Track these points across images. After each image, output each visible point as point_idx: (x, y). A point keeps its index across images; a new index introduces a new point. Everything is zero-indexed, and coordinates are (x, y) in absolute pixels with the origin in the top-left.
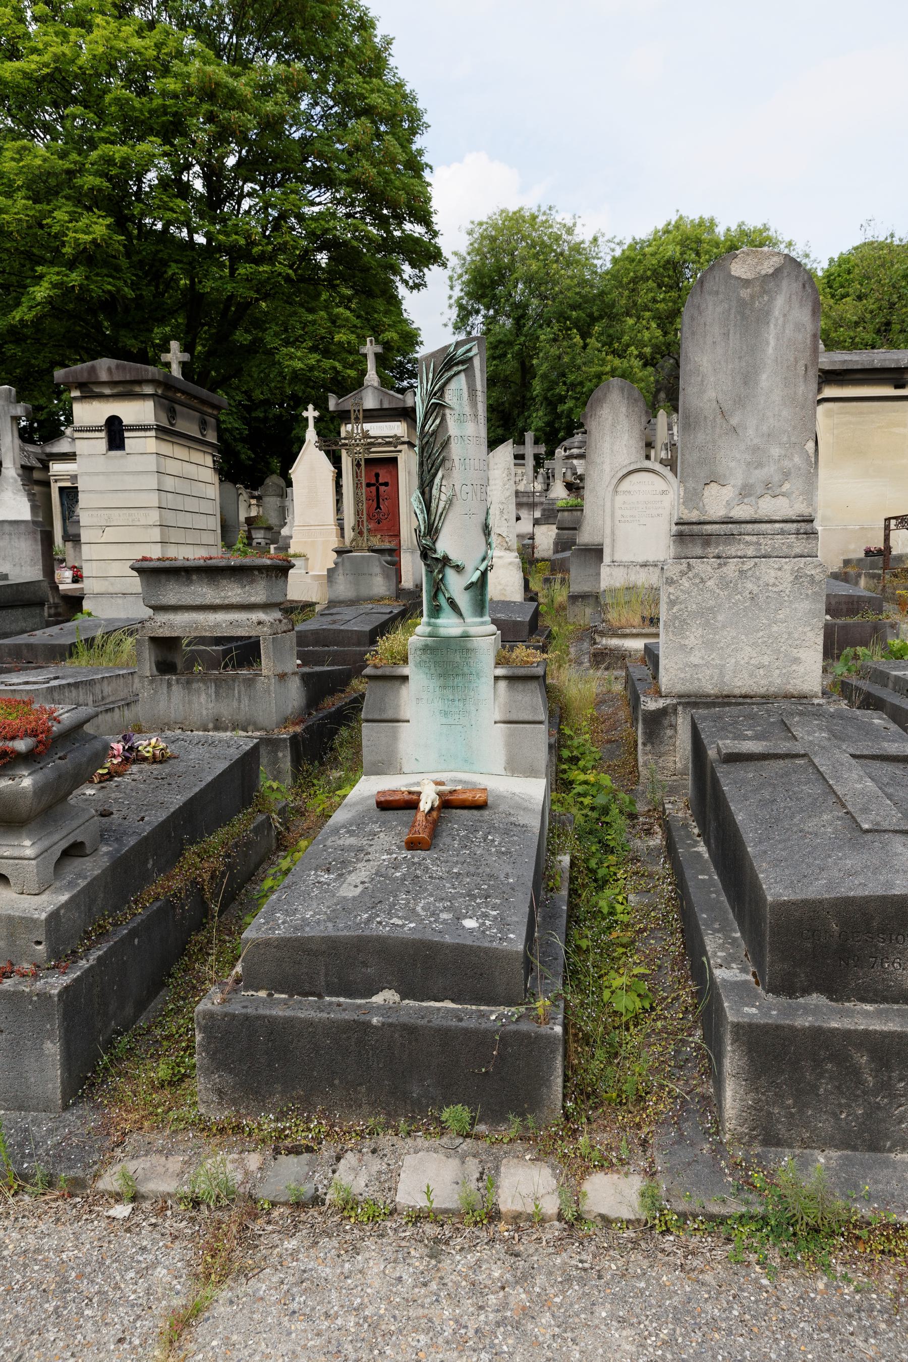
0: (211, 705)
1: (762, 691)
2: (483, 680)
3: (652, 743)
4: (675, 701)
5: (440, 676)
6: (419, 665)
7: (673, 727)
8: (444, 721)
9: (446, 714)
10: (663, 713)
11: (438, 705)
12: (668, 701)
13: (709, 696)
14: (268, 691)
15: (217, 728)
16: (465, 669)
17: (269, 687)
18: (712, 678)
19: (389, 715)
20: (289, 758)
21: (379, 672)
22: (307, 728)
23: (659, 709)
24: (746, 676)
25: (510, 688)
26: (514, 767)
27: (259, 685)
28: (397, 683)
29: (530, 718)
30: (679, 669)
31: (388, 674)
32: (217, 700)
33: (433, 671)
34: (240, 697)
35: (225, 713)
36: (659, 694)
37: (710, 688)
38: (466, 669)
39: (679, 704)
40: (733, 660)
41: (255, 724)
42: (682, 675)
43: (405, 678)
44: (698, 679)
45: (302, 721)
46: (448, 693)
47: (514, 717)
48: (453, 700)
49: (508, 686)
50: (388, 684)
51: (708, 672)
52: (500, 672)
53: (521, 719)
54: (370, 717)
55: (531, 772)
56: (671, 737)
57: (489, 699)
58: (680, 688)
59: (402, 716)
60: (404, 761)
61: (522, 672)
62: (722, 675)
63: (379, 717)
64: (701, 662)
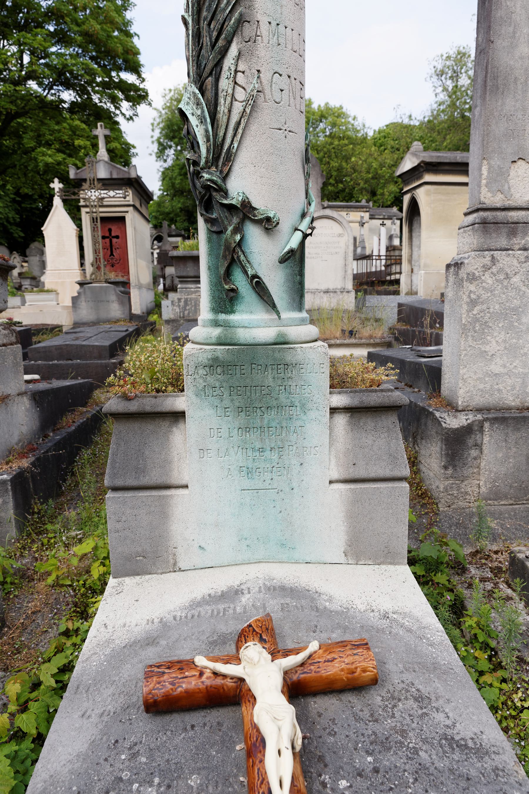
2: (312, 414)
3: (454, 467)
4: (479, 417)
5: (240, 410)
7: (479, 446)
8: (246, 483)
9: (249, 472)
10: (468, 430)
11: (236, 458)
12: (471, 417)
13: (509, 409)
18: (513, 388)
20: (11, 504)
21: (133, 407)
22: (38, 459)
23: (463, 427)
25: (353, 426)
26: (361, 549)
28: (165, 424)
30: (478, 379)
31: (148, 409)
33: (227, 402)
36: (452, 407)
37: (511, 400)
38: (283, 398)
42: (481, 386)
43: (179, 416)
44: (499, 390)
45: (33, 450)
46: (253, 437)
47: (362, 473)
48: (261, 450)
49: (350, 423)
50: (149, 427)
51: (510, 382)
52: (339, 400)
54: (119, 483)
55: (385, 557)
56: (475, 459)
57: (322, 444)
58: (479, 401)
59: (175, 479)
60: (180, 551)
61: (374, 399)
64: (502, 370)
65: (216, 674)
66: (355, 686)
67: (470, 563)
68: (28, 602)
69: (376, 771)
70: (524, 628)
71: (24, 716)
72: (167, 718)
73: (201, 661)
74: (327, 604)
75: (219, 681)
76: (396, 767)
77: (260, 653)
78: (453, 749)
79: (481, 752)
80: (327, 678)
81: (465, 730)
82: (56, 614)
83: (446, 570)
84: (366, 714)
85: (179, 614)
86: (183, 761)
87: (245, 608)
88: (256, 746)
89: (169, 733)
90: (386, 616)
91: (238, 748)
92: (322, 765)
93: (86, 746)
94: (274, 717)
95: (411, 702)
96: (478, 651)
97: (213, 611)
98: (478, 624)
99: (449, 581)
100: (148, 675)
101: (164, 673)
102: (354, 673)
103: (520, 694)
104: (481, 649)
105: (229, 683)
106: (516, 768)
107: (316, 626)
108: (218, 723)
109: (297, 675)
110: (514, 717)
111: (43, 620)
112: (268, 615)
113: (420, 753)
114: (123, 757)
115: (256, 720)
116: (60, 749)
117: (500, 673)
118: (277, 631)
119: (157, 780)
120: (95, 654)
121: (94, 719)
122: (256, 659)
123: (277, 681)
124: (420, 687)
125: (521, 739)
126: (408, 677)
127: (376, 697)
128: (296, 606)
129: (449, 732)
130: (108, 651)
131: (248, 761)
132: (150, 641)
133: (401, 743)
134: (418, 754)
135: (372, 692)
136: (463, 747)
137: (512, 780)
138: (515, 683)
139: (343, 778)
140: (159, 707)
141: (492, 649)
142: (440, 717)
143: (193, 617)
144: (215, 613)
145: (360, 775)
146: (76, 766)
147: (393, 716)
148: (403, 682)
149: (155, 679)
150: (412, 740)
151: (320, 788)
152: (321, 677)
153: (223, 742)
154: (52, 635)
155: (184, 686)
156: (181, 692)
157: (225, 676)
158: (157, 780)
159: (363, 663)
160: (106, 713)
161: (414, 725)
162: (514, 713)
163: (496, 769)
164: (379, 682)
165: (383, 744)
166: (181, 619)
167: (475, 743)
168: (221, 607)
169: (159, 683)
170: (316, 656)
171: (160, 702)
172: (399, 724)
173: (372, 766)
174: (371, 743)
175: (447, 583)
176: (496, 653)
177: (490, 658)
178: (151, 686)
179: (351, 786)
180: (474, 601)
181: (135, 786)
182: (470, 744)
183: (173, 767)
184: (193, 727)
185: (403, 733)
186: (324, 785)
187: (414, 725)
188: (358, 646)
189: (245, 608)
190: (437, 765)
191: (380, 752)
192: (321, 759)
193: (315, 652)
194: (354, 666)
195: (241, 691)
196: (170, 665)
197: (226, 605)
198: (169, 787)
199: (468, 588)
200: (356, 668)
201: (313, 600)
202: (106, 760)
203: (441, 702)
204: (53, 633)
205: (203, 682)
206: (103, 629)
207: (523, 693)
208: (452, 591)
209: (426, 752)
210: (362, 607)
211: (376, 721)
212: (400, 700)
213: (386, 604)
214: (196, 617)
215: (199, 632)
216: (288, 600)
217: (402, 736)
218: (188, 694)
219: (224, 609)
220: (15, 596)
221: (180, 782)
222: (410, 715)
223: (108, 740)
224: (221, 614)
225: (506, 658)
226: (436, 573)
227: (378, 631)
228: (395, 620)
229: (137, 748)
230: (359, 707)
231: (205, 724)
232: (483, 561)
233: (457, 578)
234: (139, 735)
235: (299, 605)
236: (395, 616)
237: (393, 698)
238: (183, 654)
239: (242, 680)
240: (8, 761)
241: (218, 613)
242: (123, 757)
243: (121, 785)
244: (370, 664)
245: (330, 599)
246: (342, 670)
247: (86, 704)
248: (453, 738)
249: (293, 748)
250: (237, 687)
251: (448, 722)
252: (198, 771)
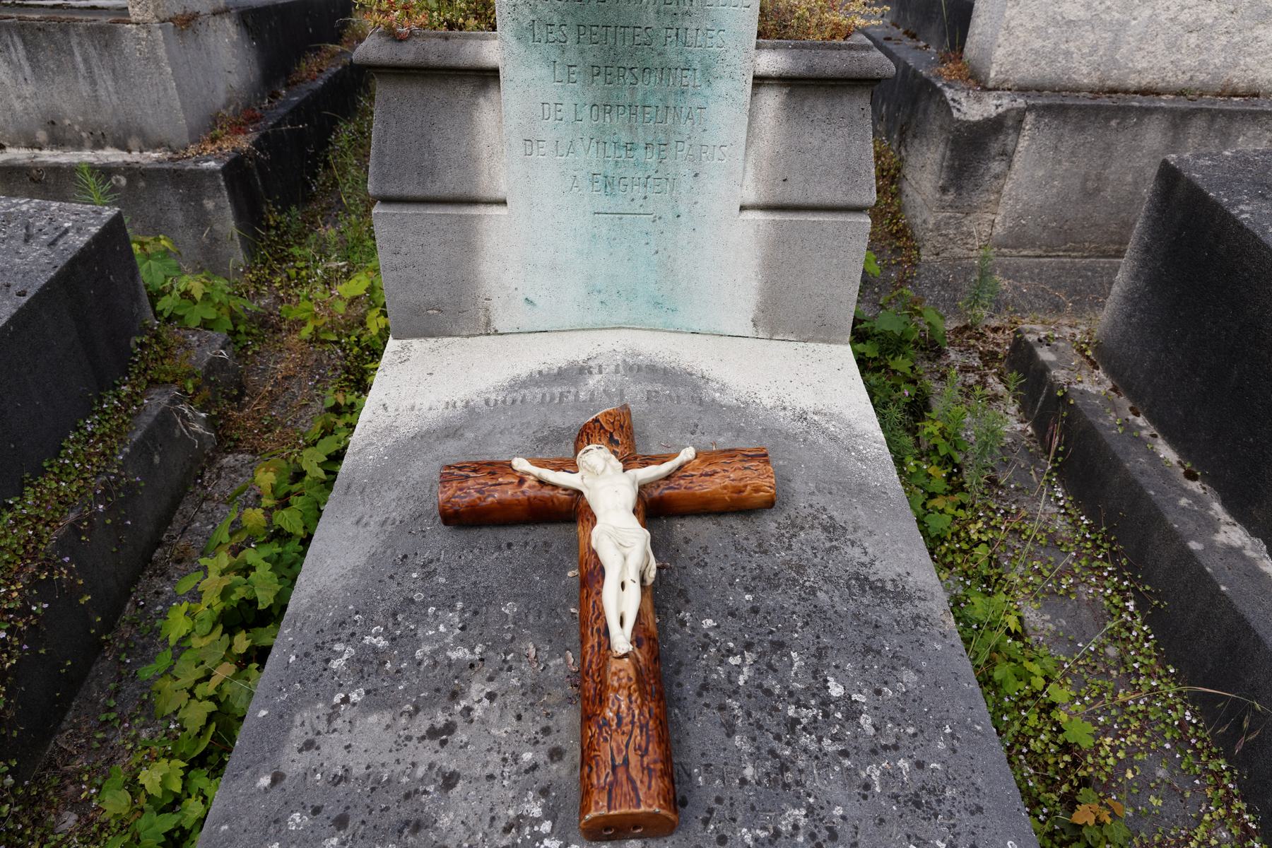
0: (28, 90)
1: (1182, 80)
2: (722, 86)
3: (959, 189)
4: (1021, 103)
5: (595, 71)
6: (527, 34)
7: (1007, 156)
8: (604, 202)
9: (609, 184)
10: (995, 126)
11: (587, 158)
12: (1006, 103)
13: (1077, 90)
14: (152, 58)
15: (57, 142)
16: (671, 50)
17: (153, 50)
18: (1094, 48)
19: (447, 184)
20: (229, 212)
21: (407, 54)
22: (264, 137)
23: (987, 120)
24: (1161, 47)
25: (791, 111)
26: (779, 317)
27: (128, 46)
28: (464, 90)
29: (839, 198)
30: (1037, 29)
31: (433, 60)
32: (39, 79)
33: (572, 56)
34: (90, 70)
35: (67, 108)
36: (977, 82)
37: (1084, 73)
38: (672, 54)
39: (1030, 108)
40: (1148, 12)
41: (142, 134)
42: (1037, 44)
43: (488, 77)
44: (1068, 54)
45: (253, 119)
46: (615, 121)
47: (795, 195)
48: (630, 147)
49: (786, 106)
50: (438, 94)
51: (1090, 37)
52: (771, 62)
53: (813, 200)
54: (393, 190)
55: (818, 332)
56: (997, 177)
58: (1027, 71)
59: (485, 189)
60: (496, 304)
61: (834, 63)
62: (1115, 44)
63: (418, 192)
64: (1083, 14)
65: (542, 483)
66: (740, 507)
67: (951, 344)
68: (276, 363)
69: (755, 610)
70: (1009, 440)
71: (285, 512)
72: (475, 533)
73: (521, 464)
74: (718, 395)
75: (547, 492)
76: (782, 608)
77: (606, 460)
78: (865, 591)
79: (901, 596)
80: (702, 496)
81: (885, 570)
82: (318, 381)
83: (912, 353)
84: (753, 543)
85: (493, 397)
86: (495, 585)
87: (592, 394)
88: (593, 574)
89: (476, 551)
90: (802, 417)
91: (570, 574)
92: (682, 601)
93: (364, 559)
94: (620, 543)
95: (818, 533)
96: (935, 467)
97: (544, 395)
98: (942, 431)
99: (913, 368)
100: (445, 479)
101: (468, 477)
102: (741, 492)
103: (980, 525)
104: (939, 464)
105: (561, 495)
106: (943, 618)
107: (696, 426)
108: (545, 543)
109: (659, 490)
110: (965, 552)
111: (300, 389)
112: (625, 407)
113: (818, 594)
114: (415, 575)
115: (593, 544)
116: (329, 561)
117: (959, 497)
118: (636, 430)
119: (459, 605)
120: (371, 444)
121: (373, 527)
122: (600, 467)
123: (628, 496)
124: (835, 514)
125: (967, 577)
126: (819, 500)
127: (770, 524)
128: (669, 396)
129: (863, 571)
130: (390, 442)
131: (581, 591)
132: (450, 431)
133: (794, 580)
134: (815, 595)
135: (765, 516)
136: (878, 589)
137: (935, 631)
138: (976, 510)
139: (709, 617)
141: (955, 466)
142: (855, 552)
143: (514, 402)
144: (548, 399)
145: (732, 614)
146: (351, 582)
147: (790, 548)
148: (811, 506)
149: (455, 484)
150: (811, 578)
151: (677, 626)
152: (694, 494)
153: (550, 566)
154: (314, 410)
155: (496, 495)
156: (492, 503)
157: (555, 487)
158: (459, 605)
159: (758, 480)
160: (389, 522)
161: (816, 561)
162: (965, 547)
163: (916, 618)
164: (777, 503)
165: (771, 581)
166: (496, 404)
167: (896, 586)
168: (557, 390)
169: (461, 490)
170: (689, 467)
171: (463, 513)
172: (795, 558)
173: (750, 606)
174: (754, 579)
175: (908, 372)
176: (960, 471)
177: (949, 478)
178: (450, 493)
179: (718, 626)
180: (943, 399)
181: (431, 610)
182: (889, 586)
183: (482, 591)
184: (509, 545)
185: (800, 569)
186: (683, 623)
187: (816, 561)
188: (753, 458)
189: (592, 394)
190: (838, 609)
191: (764, 590)
192: (682, 593)
193: (689, 462)
194: (742, 483)
195: (577, 505)
196: (477, 467)
197: (565, 389)
198: (476, 613)
199: (940, 379)
200: (746, 486)
201: (696, 387)
202: (391, 577)
203: (860, 534)
204: (317, 407)
205: (523, 492)
206: (381, 411)
207: (984, 523)
208: (914, 382)
209: (827, 592)
210: (768, 403)
211: (765, 552)
212: (802, 528)
213: (805, 401)
214: (518, 402)
215: (522, 424)
216: (658, 387)
217: (798, 573)
218: (502, 505)
219: (561, 394)
220: (254, 352)
221: (491, 609)
222: (813, 548)
223: (393, 554)
224: (557, 401)
225: (971, 477)
226: (896, 355)
227: (787, 437)
228: (815, 423)
229: (433, 566)
230: (744, 535)
231: (526, 544)
232: (972, 342)
233: (926, 364)
234: (435, 551)
235: (674, 395)
236: (816, 418)
237: (793, 525)
238: (496, 452)
239: (579, 493)
240: (269, 566)
241: (552, 399)
242: (415, 575)
243: (413, 607)
244: (766, 483)
245: (723, 389)
246: (725, 487)
247: (361, 508)
248: (866, 579)
249: (643, 580)
250: (572, 501)
251: (865, 559)
252: (515, 598)
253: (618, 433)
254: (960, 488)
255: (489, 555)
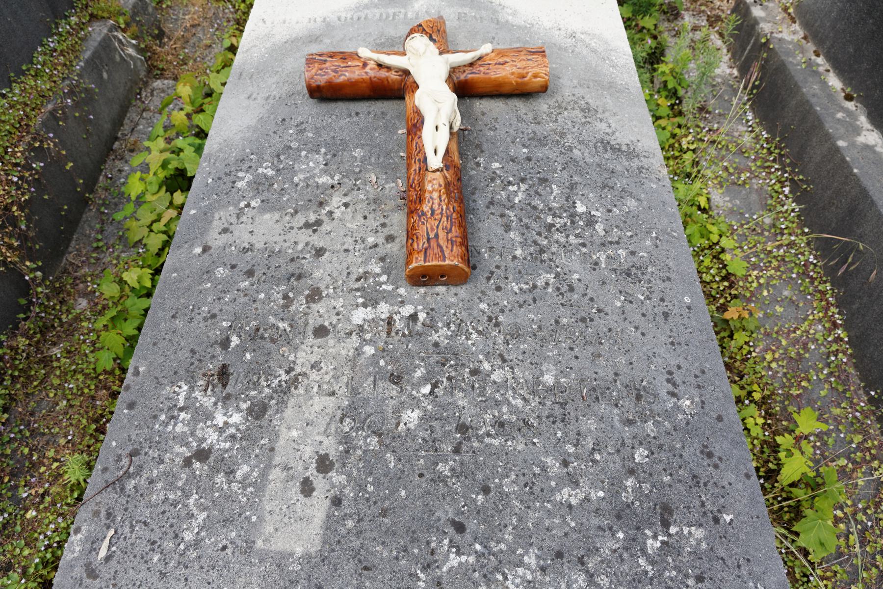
65: (380, 66)
66: (523, 92)
67: (687, 10)
68: (184, 14)
69: (529, 159)
70: (719, 80)
71: (201, 116)
72: (333, 105)
73: (365, 52)
74: (510, 18)
75: (383, 74)
76: (548, 158)
77: (427, 46)
78: (606, 150)
79: (631, 154)
80: (495, 80)
81: (622, 138)
82: (217, 29)
83: (656, 14)
84: (530, 117)
85: (343, 15)
86: (347, 138)
87: (417, 14)
88: (415, 125)
89: (334, 117)
90: (572, 36)
91: (400, 132)
92: (479, 151)
93: (255, 121)
94: (437, 107)
95: (577, 112)
96: (663, 99)
97: (381, 15)
98: (672, 71)
99: (656, 25)
100: (310, 61)
101: (326, 61)
102: (524, 77)
103: (690, 138)
104: (666, 97)
105: (393, 76)
106: (660, 169)
107: (494, 38)
108: (383, 113)
109: (465, 74)
110: (676, 158)
111: (204, 35)
112: (441, 17)
113: (574, 151)
114: (291, 132)
115: (417, 103)
116: (230, 122)
117: (678, 120)
118: (450, 39)
119: (323, 150)
120: (255, 46)
121: (260, 100)
122: (422, 50)
123: (444, 73)
124: (590, 101)
125: (676, 174)
126: (580, 92)
127: (542, 105)
128: (475, 17)
129: (607, 138)
130: (268, 45)
131: (408, 138)
132: (314, 39)
133: (558, 141)
134: (571, 151)
135: (540, 100)
136: (617, 150)
137: (653, 177)
138: (688, 128)
139: (497, 161)
140: (325, 94)
141: (678, 98)
142: (603, 126)
143: (359, 19)
144: (384, 17)
145: (513, 161)
146: (247, 135)
147: (556, 121)
148: (574, 95)
149: (316, 65)
150: (570, 140)
151: (474, 166)
152: (490, 78)
153: (386, 127)
154: (216, 50)
155: (347, 74)
156: (345, 81)
157: (389, 68)
158: (323, 150)
160: (271, 97)
161: (574, 130)
162: (677, 154)
163: (640, 169)
164: (548, 92)
165: (542, 142)
166: (346, 20)
167: (629, 148)
169: (321, 69)
170: (488, 58)
171: (323, 87)
172: (559, 128)
173: (525, 156)
174: (529, 140)
175: (652, 28)
176: (681, 102)
177: (672, 107)
178: (313, 71)
179: (503, 168)
180: (676, 50)
181: (304, 153)
182: (624, 148)
183: (338, 142)
184: (357, 114)
185: (562, 135)
186: (478, 164)
187: (574, 130)
188: (534, 53)
189: (417, 14)
190: (587, 160)
191: (536, 146)
192: (479, 146)
193: (487, 55)
194: (525, 71)
195: (405, 84)
196: (332, 55)
197: (397, 10)
198: (334, 155)
199: (675, 36)
200: (527, 73)
201: (495, 12)
202: (275, 132)
203: (607, 114)
204: (217, 49)
205: (366, 73)
206: (261, 24)
207: (694, 137)
208: (655, 37)
209: (580, 150)
210: (548, 25)
211: (539, 123)
212: (566, 109)
213: (575, 24)
214: (362, 19)
215: (366, 34)
216: (466, 10)
217: (560, 137)
218: (353, 84)
219: (394, 14)
220: (168, 6)
221: (345, 154)
222: (572, 122)
223: (275, 118)
224: (391, 18)
225: (688, 106)
226: (644, 16)
227: (560, 48)
228: (582, 40)
229: (303, 126)
230: (524, 111)
231: (369, 113)
232: (703, 8)
233: (666, 24)
234: (305, 116)
235: (478, 16)
236: (583, 36)
237: (560, 107)
238: (348, 48)
239: (406, 73)
240: (193, 149)
241: (388, 17)
242: (291, 132)
243: (291, 151)
244: (542, 71)
245: (514, 14)
246: (513, 74)
247: (250, 88)
248: (609, 143)
249: (451, 128)
250: (402, 81)
251: (609, 131)
252: (362, 146)
253: (435, 32)
254: (680, 114)
255: (343, 118)
